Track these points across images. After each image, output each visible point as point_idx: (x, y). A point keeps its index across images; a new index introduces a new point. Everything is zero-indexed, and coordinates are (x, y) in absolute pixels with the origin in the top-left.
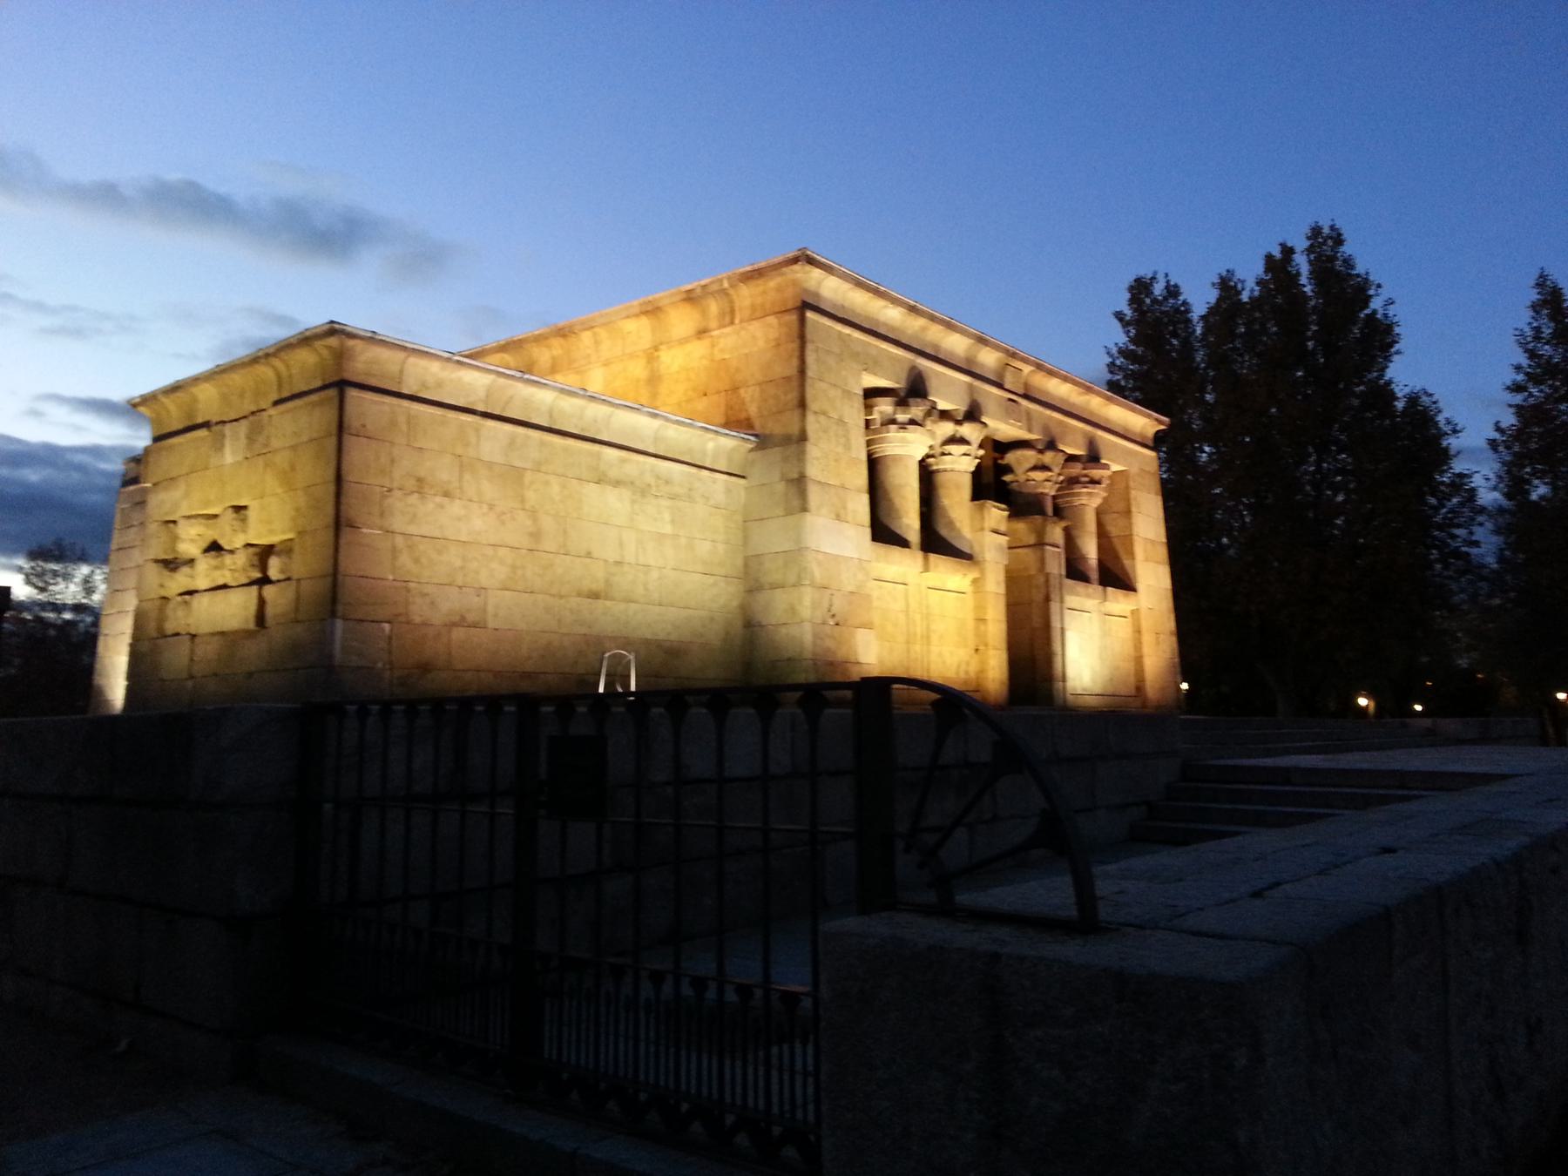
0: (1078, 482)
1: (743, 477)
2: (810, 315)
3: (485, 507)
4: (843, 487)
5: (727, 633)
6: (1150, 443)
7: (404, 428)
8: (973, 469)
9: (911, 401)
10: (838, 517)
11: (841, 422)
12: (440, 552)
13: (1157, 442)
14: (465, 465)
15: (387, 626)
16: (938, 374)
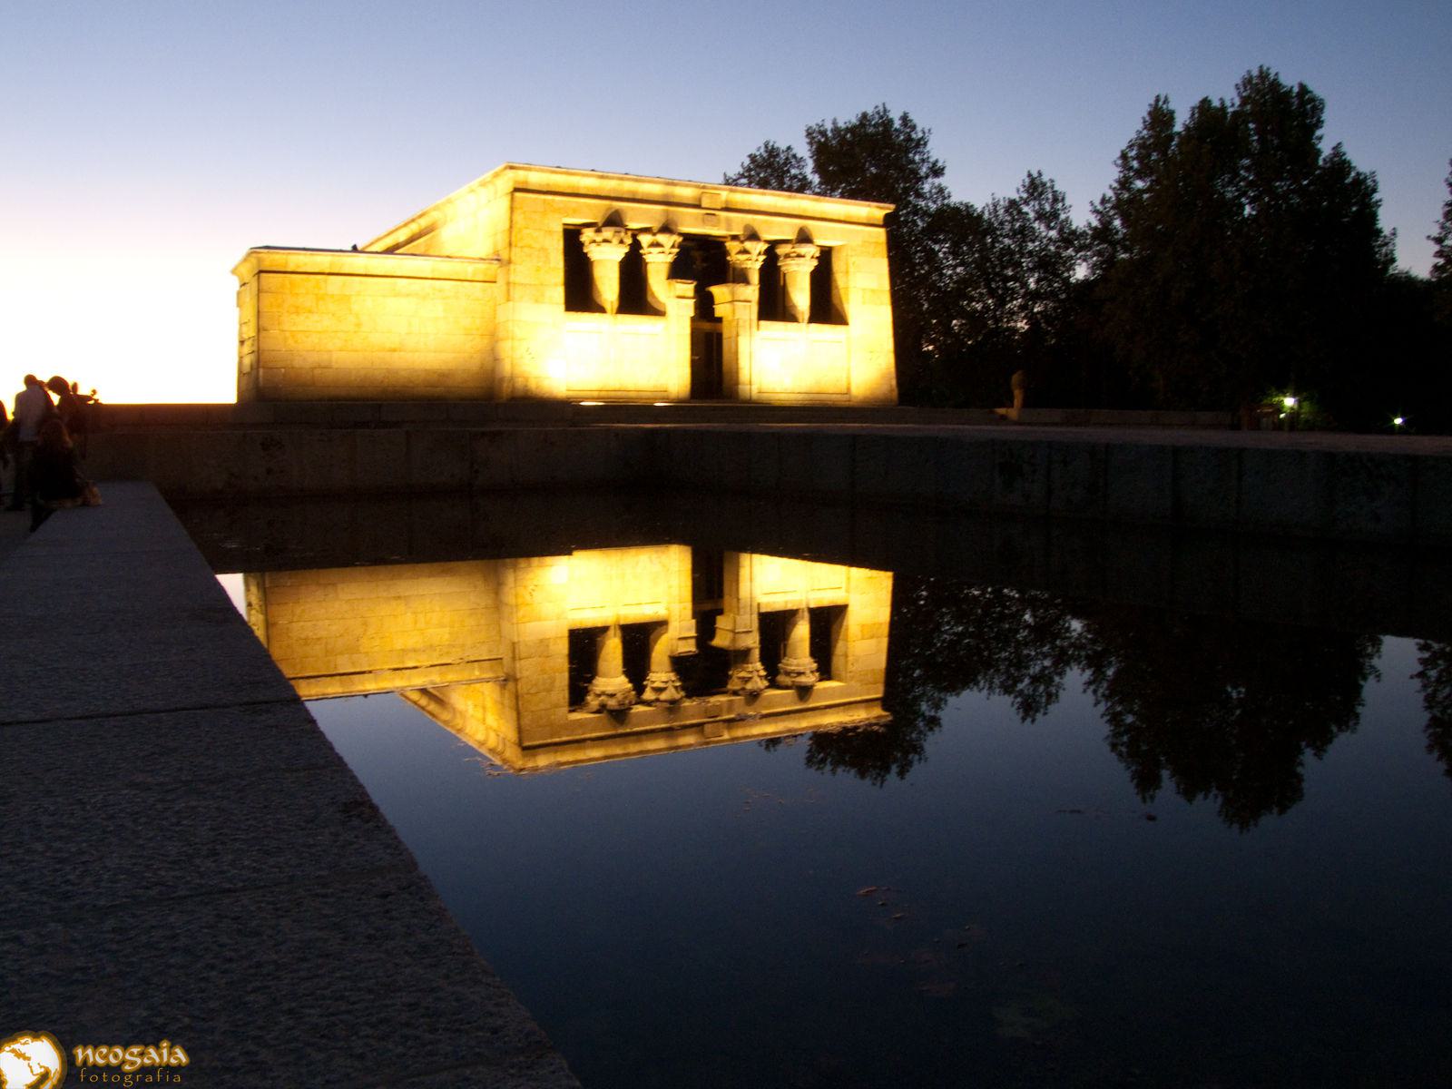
0: (790, 257)
1: (495, 282)
2: (518, 195)
3: (330, 315)
4: (542, 284)
5: (482, 364)
6: (881, 223)
7: (288, 286)
8: (672, 261)
9: (603, 229)
10: (537, 301)
11: (543, 249)
12: (307, 337)
13: (889, 222)
14: (319, 298)
15: (283, 370)
16: (632, 209)
